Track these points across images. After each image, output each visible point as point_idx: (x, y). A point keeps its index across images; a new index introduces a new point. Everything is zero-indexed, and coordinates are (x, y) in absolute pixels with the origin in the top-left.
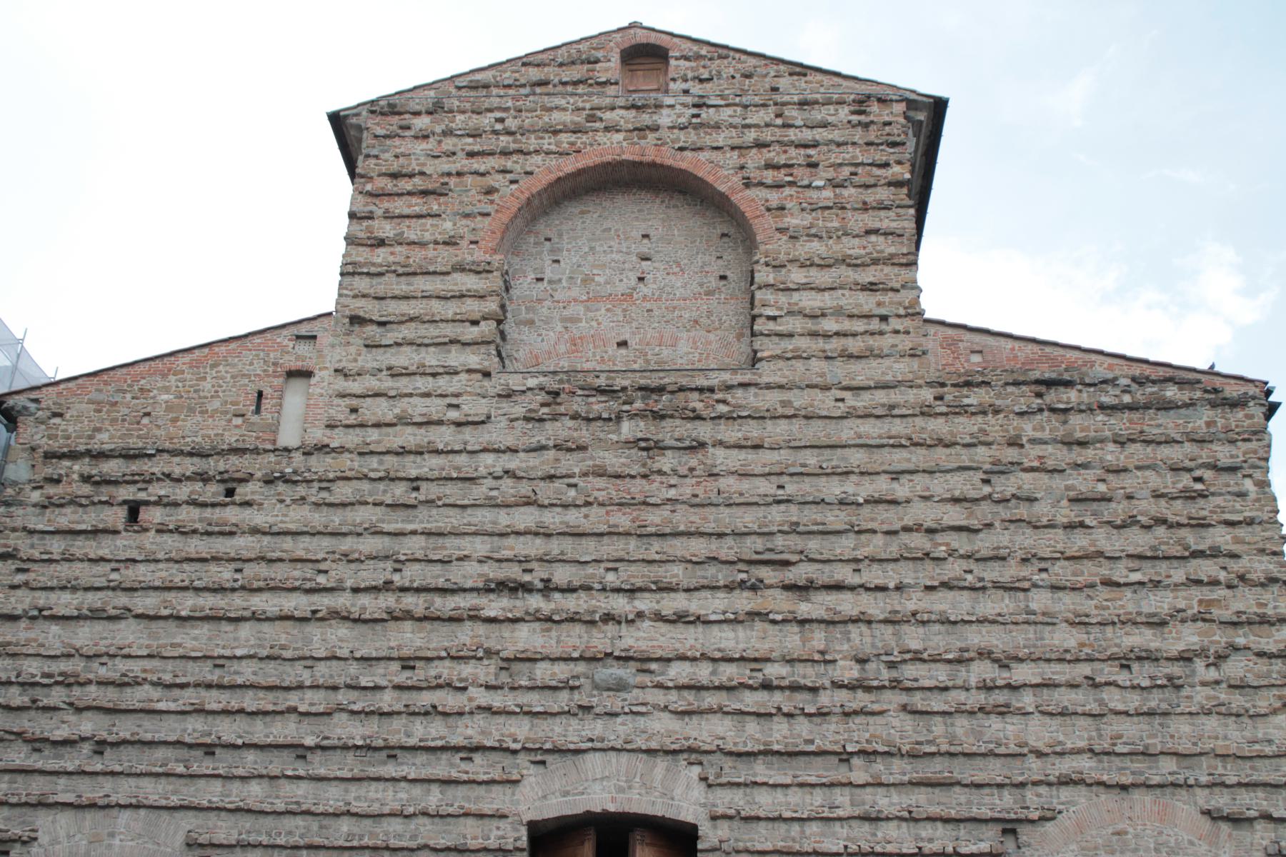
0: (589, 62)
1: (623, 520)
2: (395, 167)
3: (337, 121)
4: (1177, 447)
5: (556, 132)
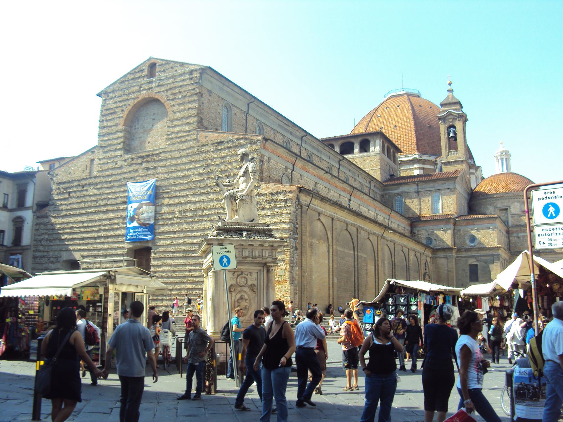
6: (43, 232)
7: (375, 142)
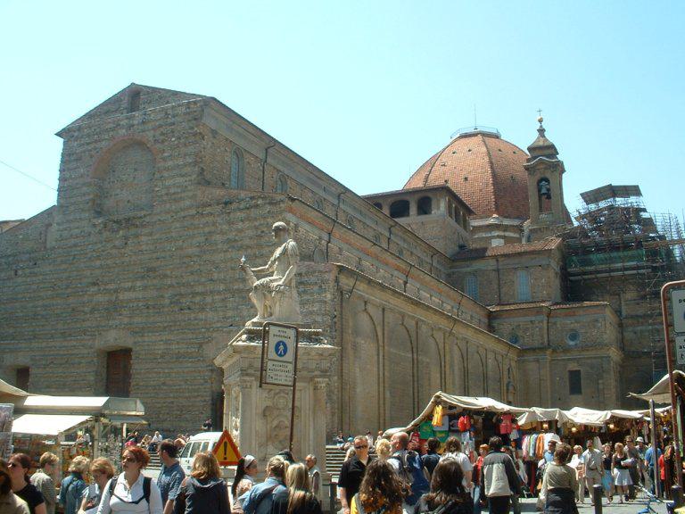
7: (438, 200)
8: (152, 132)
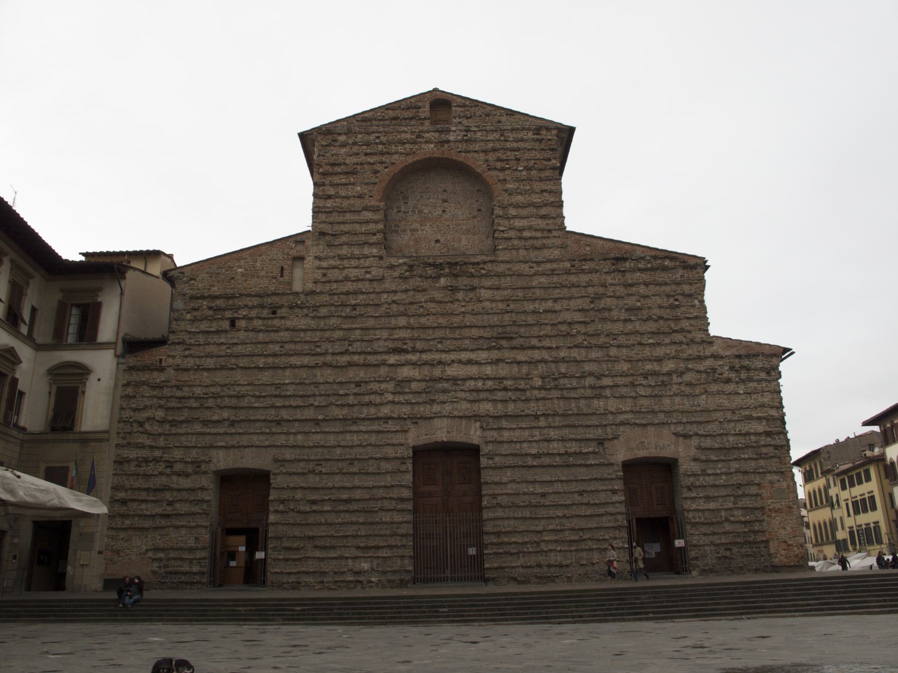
0: (416, 108)
1: (442, 321)
2: (332, 160)
3: (303, 136)
4: (669, 287)
5: (404, 144)
6: (148, 402)
8: (482, 156)
